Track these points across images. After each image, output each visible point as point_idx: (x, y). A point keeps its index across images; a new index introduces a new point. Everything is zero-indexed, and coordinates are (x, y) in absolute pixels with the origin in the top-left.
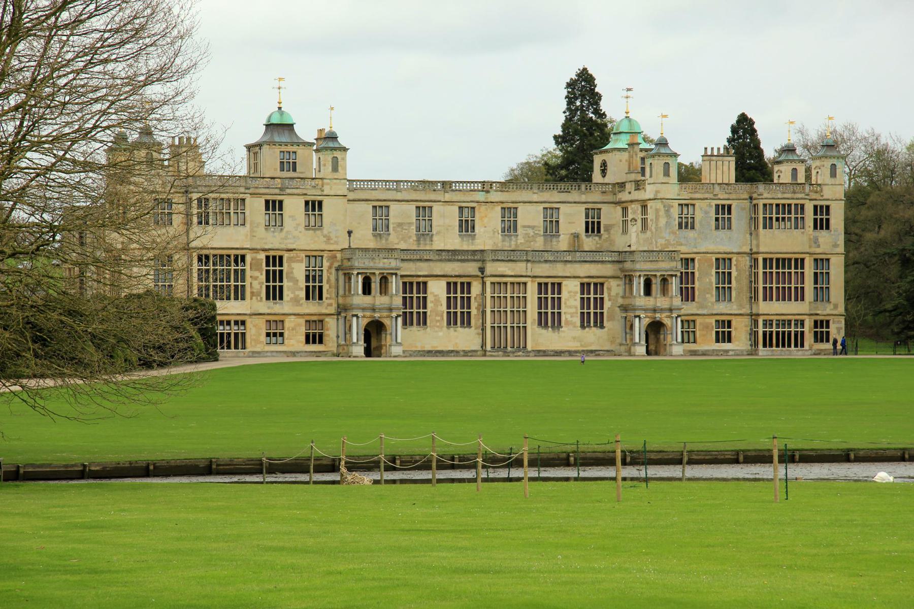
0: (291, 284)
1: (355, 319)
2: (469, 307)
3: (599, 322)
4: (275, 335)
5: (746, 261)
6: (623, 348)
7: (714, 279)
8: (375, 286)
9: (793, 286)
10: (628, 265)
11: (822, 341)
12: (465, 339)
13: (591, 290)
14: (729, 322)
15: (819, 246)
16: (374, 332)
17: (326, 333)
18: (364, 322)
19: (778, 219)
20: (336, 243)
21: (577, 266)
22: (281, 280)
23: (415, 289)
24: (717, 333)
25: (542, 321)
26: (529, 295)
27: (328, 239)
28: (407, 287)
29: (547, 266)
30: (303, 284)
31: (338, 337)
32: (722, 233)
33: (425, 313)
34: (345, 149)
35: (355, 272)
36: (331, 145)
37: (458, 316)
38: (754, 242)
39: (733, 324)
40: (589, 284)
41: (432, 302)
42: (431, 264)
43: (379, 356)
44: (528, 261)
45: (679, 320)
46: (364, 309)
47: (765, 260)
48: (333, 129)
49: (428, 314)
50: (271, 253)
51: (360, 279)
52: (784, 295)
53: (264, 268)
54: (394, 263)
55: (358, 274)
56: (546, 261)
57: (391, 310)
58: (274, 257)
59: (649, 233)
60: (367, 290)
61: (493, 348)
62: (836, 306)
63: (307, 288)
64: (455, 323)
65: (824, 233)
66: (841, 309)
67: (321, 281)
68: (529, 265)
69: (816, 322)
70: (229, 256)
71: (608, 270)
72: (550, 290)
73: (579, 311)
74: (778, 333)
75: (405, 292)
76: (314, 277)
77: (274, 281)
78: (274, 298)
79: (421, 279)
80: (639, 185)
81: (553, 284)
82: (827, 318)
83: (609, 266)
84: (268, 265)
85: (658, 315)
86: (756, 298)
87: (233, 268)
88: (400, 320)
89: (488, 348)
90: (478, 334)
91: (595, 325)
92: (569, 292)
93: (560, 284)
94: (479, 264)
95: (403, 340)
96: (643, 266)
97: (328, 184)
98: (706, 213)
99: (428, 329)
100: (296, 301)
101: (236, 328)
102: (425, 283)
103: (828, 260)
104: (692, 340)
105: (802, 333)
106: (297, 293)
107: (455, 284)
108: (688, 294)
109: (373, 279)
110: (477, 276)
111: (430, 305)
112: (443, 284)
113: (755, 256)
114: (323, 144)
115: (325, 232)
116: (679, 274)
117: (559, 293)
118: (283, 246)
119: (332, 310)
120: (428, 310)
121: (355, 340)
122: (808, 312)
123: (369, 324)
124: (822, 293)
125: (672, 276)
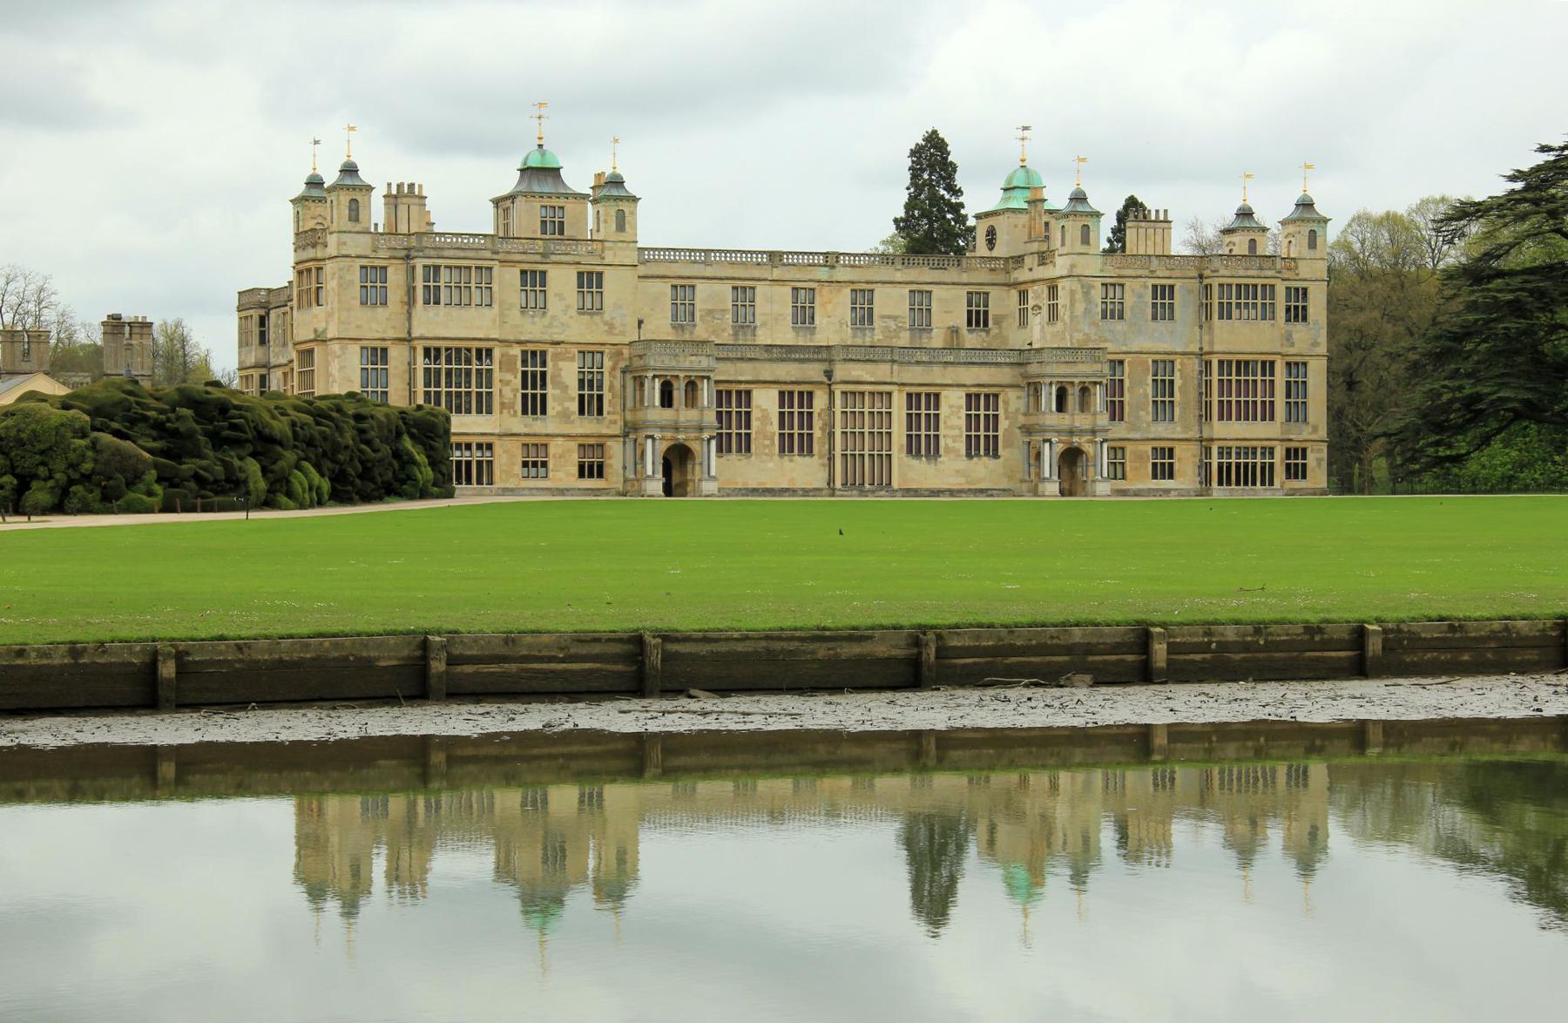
1: (649, 442)
2: (810, 427)
3: (992, 450)
4: (535, 464)
5: (1194, 365)
6: (1025, 486)
7: (1150, 390)
8: (679, 395)
9: (1259, 399)
10: (1033, 369)
12: (805, 471)
13: (981, 402)
14: (1171, 450)
15: (1292, 345)
16: (677, 460)
17: (607, 462)
18: (662, 447)
19: (1238, 305)
20: (623, 333)
21: (962, 369)
22: (544, 386)
23: (734, 400)
24: (1154, 465)
25: (912, 448)
26: (894, 410)
27: (611, 327)
28: (722, 397)
29: (919, 369)
31: (625, 468)
32: (1161, 325)
33: (748, 435)
34: (635, 199)
36: (615, 192)
37: (794, 442)
38: (1206, 338)
39: (1177, 452)
40: (978, 396)
42: (758, 365)
44: (893, 361)
46: (662, 428)
47: (1221, 362)
48: (618, 171)
50: (530, 347)
52: (1246, 413)
53: (520, 368)
54: (705, 362)
55: (655, 377)
56: (918, 363)
57: (701, 429)
59: (1059, 325)
60: (667, 400)
61: (844, 484)
63: (581, 397)
64: (791, 450)
65: (1300, 326)
67: (600, 387)
70: (469, 350)
71: (1004, 375)
72: (924, 403)
74: (1238, 465)
75: (720, 405)
76: (591, 382)
78: (534, 412)
79: (742, 387)
80: (1044, 258)
81: (928, 395)
83: (1006, 370)
84: (524, 363)
85: (1075, 439)
86: (1208, 417)
88: (713, 443)
89: (838, 485)
91: (987, 454)
93: (937, 396)
94: (825, 366)
95: (717, 472)
100: (564, 416)
102: (748, 393)
103: (1305, 364)
104: (1119, 475)
105: (1272, 465)
106: (567, 404)
107: (791, 393)
108: (1116, 411)
109: (675, 385)
111: (755, 424)
112: (773, 393)
113: (1207, 357)
114: (605, 192)
115: (607, 317)
117: (937, 407)
118: (547, 338)
119: (616, 429)
120: (753, 431)
121: (650, 472)
124: (1297, 411)
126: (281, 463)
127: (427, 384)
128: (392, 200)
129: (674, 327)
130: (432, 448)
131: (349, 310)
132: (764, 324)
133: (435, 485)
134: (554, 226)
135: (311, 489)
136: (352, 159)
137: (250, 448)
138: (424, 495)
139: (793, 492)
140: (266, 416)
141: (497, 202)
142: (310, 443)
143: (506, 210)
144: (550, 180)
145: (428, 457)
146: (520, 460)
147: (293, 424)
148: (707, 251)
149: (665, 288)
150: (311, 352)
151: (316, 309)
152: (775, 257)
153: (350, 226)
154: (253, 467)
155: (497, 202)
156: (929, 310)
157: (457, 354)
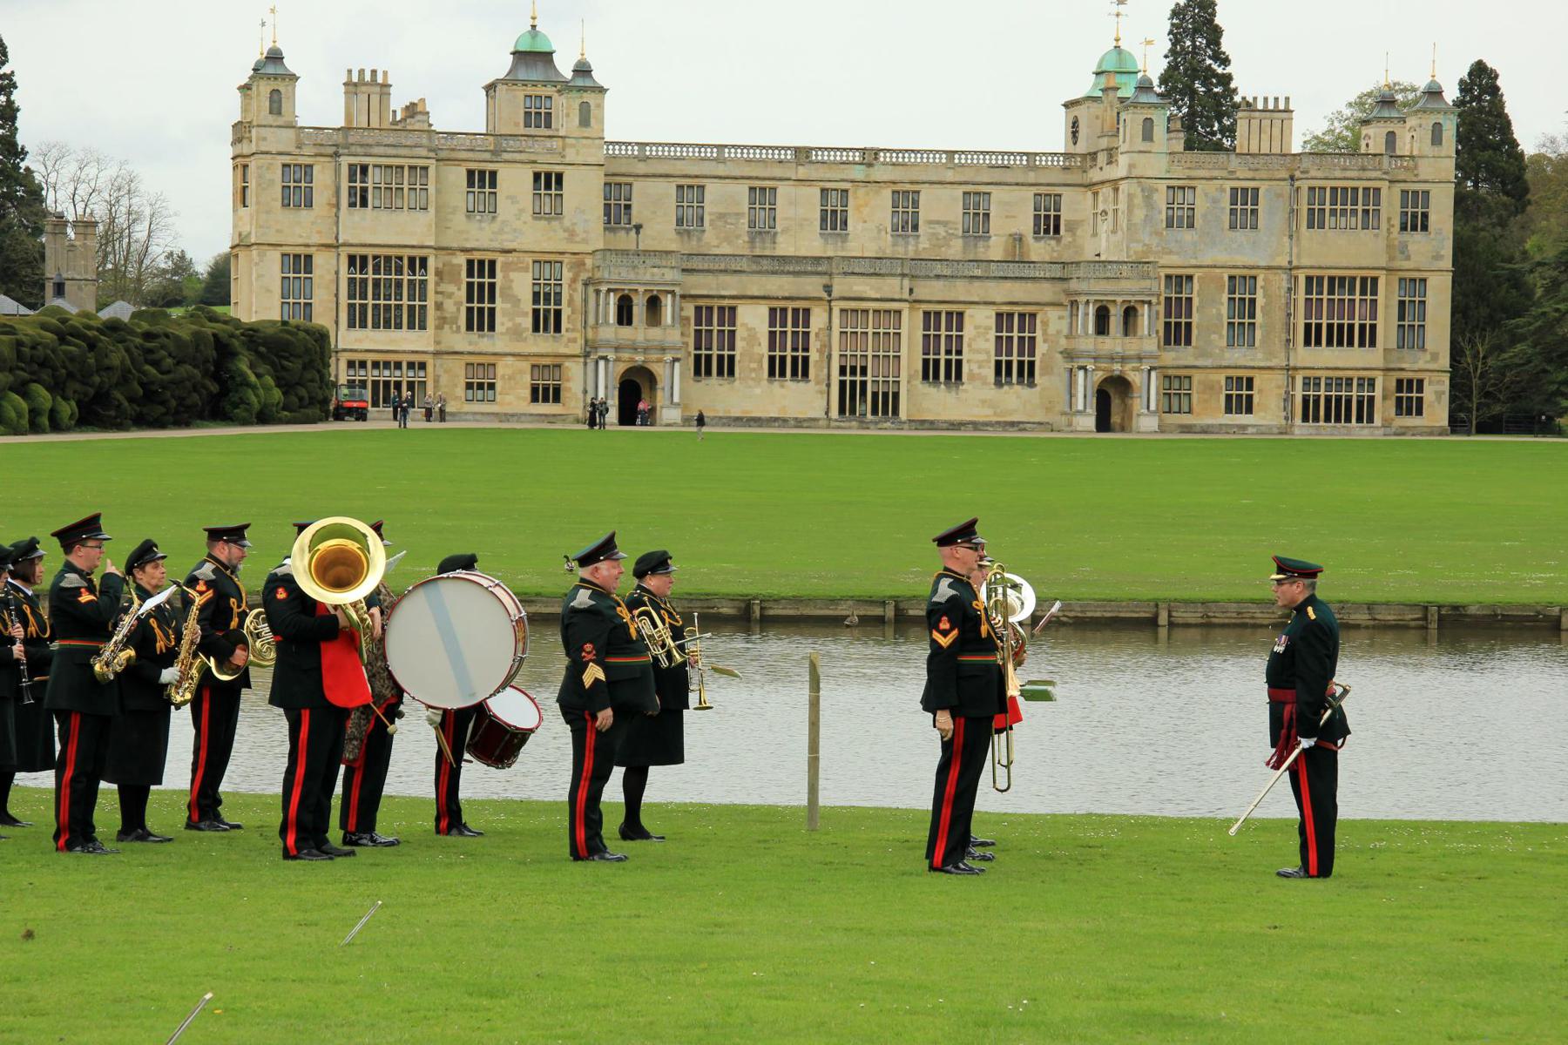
3: (1027, 373)
13: (1015, 324)
17: (564, 385)
19: (1333, 212)
20: (585, 241)
21: (991, 284)
22: (492, 299)
25: (930, 372)
27: (571, 234)
30: (528, 306)
31: (585, 392)
32: (1240, 236)
37: (788, 365)
40: (1010, 315)
41: (743, 339)
43: (652, 425)
47: (1309, 279)
49: (737, 359)
50: (477, 256)
55: (609, 290)
58: (481, 263)
63: (536, 312)
64: (783, 374)
70: (401, 258)
71: (1045, 292)
73: (993, 358)
76: (547, 295)
77: (481, 300)
78: (481, 328)
81: (949, 314)
83: (1046, 285)
84: (470, 274)
91: (1019, 383)
92: (976, 327)
93: (961, 315)
98: (1215, 201)
99: (737, 383)
100: (516, 333)
101: (411, 373)
106: (518, 320)
108: (1177, 334)
111: (739, 344)
112: (763, 310)
115: (567, 223)
117: (960, 328)
118: (496, 245)
119: (577, 348)
120: (737, 353)
127: (351, 296)
129: (678, 233)
130: (284, 368)
131: (268, 212)
133: (284, 409)
139: (784, 421)
142: (44, 363)
146: (462, 382)
148: (721, 147)
152: (802, 154)
156: (987, 216)
157: (387, 263)
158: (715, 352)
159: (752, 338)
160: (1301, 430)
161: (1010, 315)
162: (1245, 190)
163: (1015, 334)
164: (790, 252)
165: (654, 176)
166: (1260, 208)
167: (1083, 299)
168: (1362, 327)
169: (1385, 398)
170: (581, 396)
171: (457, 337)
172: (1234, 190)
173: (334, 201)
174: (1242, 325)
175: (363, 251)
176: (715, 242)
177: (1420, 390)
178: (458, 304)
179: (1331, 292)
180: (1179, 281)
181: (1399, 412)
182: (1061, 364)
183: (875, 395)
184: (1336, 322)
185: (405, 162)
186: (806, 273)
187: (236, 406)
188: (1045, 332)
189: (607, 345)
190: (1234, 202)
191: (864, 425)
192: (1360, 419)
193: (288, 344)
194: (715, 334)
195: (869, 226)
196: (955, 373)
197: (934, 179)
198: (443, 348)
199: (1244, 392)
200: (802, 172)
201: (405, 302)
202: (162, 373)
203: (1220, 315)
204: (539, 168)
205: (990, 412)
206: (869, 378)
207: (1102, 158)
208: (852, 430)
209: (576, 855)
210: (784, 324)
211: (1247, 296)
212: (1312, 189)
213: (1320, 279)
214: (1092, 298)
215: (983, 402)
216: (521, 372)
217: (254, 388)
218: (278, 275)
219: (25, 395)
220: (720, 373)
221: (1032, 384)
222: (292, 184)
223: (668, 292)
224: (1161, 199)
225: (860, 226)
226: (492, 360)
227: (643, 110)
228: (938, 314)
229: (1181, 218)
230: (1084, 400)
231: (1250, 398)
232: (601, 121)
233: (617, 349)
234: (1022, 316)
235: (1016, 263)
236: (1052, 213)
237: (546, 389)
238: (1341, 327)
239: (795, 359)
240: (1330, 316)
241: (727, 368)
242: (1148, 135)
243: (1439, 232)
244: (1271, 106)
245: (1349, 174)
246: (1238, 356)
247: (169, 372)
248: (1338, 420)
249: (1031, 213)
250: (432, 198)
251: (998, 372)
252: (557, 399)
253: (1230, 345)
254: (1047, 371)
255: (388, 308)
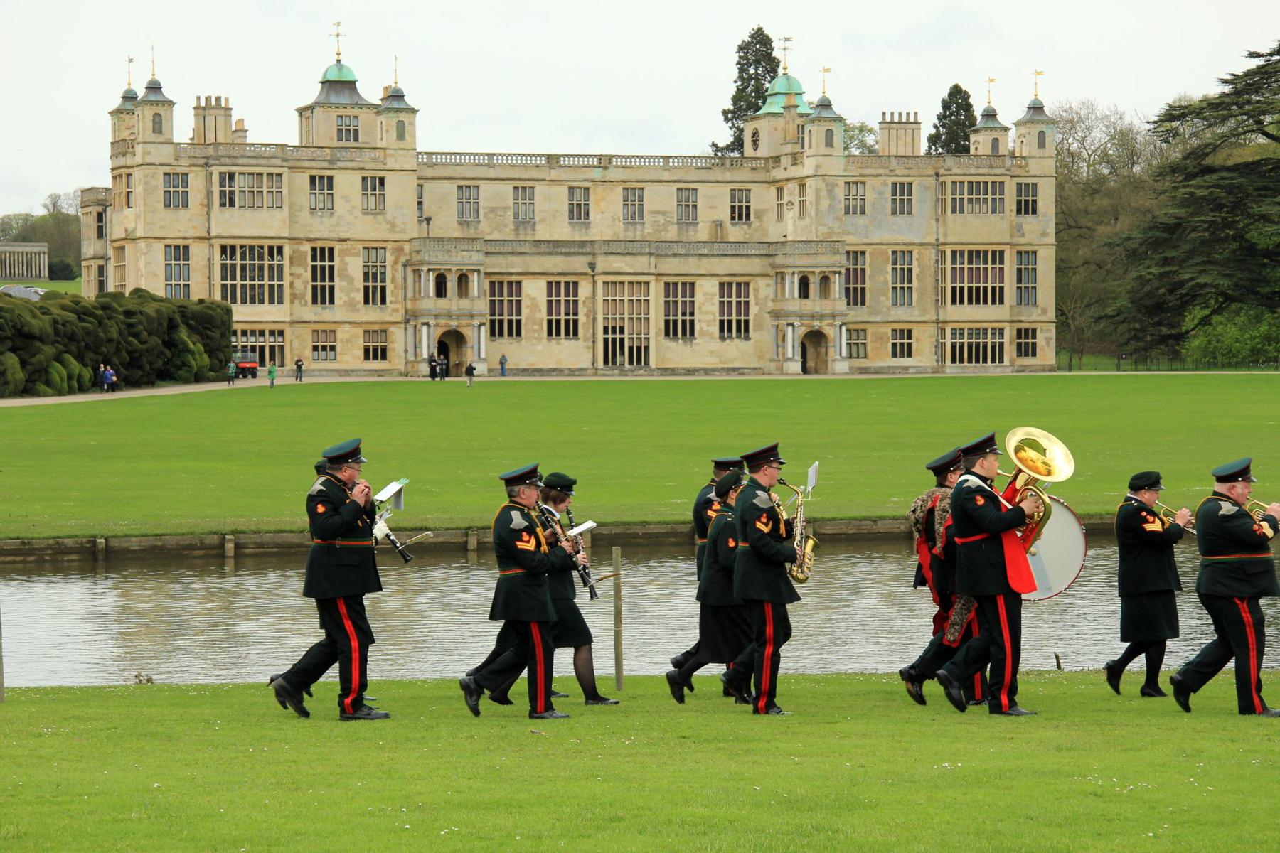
0: (344, 283)
1: (425, 328)
3: (743, 329)
4: (324, 348)
5: (931, 254)
6: (773, 366)
8: (452, 285)
10: (779, 260)
11: (1027, 355)
13: (734, 291)
14: (910, 332)
15: (1023, 235)
17: (390, 346)
19: (970, 201)
20: (403, 231)
21: (715, 261)
22: (332, 279)
23: (505, 290)
24: (894, 345)
25: (670, 330)
26: (652, 298)
27: (393, 226)
28: (495, 288)
29: (676, 260)
30: (360, 284)
31: (406, 351)
32: (899, 219)
34: (413, 111)
35: (425, 268)
36: (395, 105)
38: (941, 230)
39: (914, 334)
40: (730, 284)
42: (527, 258)
44: (651, 254)
45: (844, 328)
47: (954, 252)
48: (399, 86)
49: (523, 322)
50: (319, 244)
51: (432, 276)
52: (977, 297)
54: (476, 257)
56: (675, 255)
57: (472, 316)
58: (322, 249)
59: (807, 219)
62: (1044, 311)
63: (366, 288)
64: (558, 334)
65: (1030, 218)
66: (1051, 315)
67: (383, 280)
68: (653, 259)
69: (1019, 331)
70: (262, 247)
71: (755, 265)
73: (718, 318)
74: (970, 345)
75: (493, 294)
76: (375, 275)
77: (323, 280)
78: (323, 302)
79: (513, 278)
80: (796, 159)
81: (684, 284)
82: (1033, 326)
83: (756, 260)
84: (314, 259)
86: (943, 301)
87: (266, 262)
88: (484, 331)
90: (588, 347)
91: (739, 337)
92: (705, 294)
93: (692, 284)
96: (798, 262)
97: (392, 156)
98: (881, 193)
100: (351, 305)
101: (272, 339)
102: (519, 283)
103: (1035, 253)
104: (862, 354)
105: (1001, 345)
106: (353, 295)
108: (855, 296)
110: (586, 274)
111: (524, 311)
112: (542, 284)
113: (941, 248)
114: (387, 104)
115: (389, 217)
116: (843, 271)
117: (692, 295)
118: (335, 236)
119: (398, 317)
120: (523, 318)
122: (1008, 318)
123: (445, 334)
124: (1026, 294)
125: (835, 272)
126: (39, 357)
127: (224, 278)
128: (201, 112)
129: (460, 223)
130: (209, 337)
132: (542, 220)
133: (210, 370)
134: (349, 133)
135: (70, 377)
136: (157, 77)
137: (10, 344)
138: (199, 378)
139: (560, 371)
140: (28, 317)
141: (301, 111)
142: (72, 337)
143: (307, 118)
144: (347, 92)
145: (205, 345)
147: (55, 322)
148: (491, 155)
149: (451, 188)
150: (123, 248)
151: (127, 211)
152: (553, 160)
153: (154, 137)
154: (12, 360)
155: (301, 111)
157: (252, 251)
158: (506, 318)
159: (534, 306)
160: (951, 369)
161: (730, 284)
162: (902, 184)
163: (734, 299)
164: (547, 237)
165: (440, 178)
166: (913, 197)
167: (791, 270)
168: (994, 289)
169: (1011, 343)
170: (403, 354)
171: (304, 309)
172: (894, 184)
173: (205, 202)
174: (902, 292)
175: (232, 242)
176: (488, 230)
177: (1034, 337)
178: (306, 283)
179: (970, 262)
180: (856, 255)
181: (1019, 355)
182: (769, 322)
183: (631, 349)
184: (974, 285)
185: (264, 170)
186: (574, 254)
187: (179, 368)
188: (756, 297)
189: (428, 313)
190: (894, 194)
191: (623, 372)
192: (993, 361)
193: (211, 317)
194: (563, 303)
195: (606, 219)
196: (689, 331)
197: (655, 178)
198: (295, 319)
199: (906, 341)
200: (554, 174)
201: (266, 282)
202: (142, 343)
203: (886, 282)
204: (366, 173)
205: (717, 360)
206: (626, 336)
207: (785, 161)
208: (614, 376)
209: (531, 716)
210: (558, 294)
211: (906, 267)
212: (954, 183)
213: (962, 253)
214: (797, 270)
215: (712, 352)
216: (356, 336)
217: (192, 353)
218: (163, 263)
219: (62, 362)
220: (510, 334)
221: (747, 338)
222: (172, 189)
223: (474, 270)
224: (840, 192)
225: (599, 216)
226: (332, 327)
227: (446, 127)
228: (675, 284)
229: (855, 207)
230: (791, 347)
231: (910, 345)
232: (413, 135)
233: (437, 316)
234: (739, 284)
235: (719, 244)
236: (744, 204)
237: (375, 350)
238: (978, 289)
239: (567, 322)
240: (970, 281)
241: (515, 329)
242: (829, 143)
243: (1045, 215)
244: (904, 120)
245: (981, 171)
246: (901, 313)
247: (145, 342)
248: (977, 361)
249: (728, 204)
250: (286, 200)
251: (722, 329)
252: (384, 357)
253: (895, 304)
254: (759, 327)
255: (252, 287)
